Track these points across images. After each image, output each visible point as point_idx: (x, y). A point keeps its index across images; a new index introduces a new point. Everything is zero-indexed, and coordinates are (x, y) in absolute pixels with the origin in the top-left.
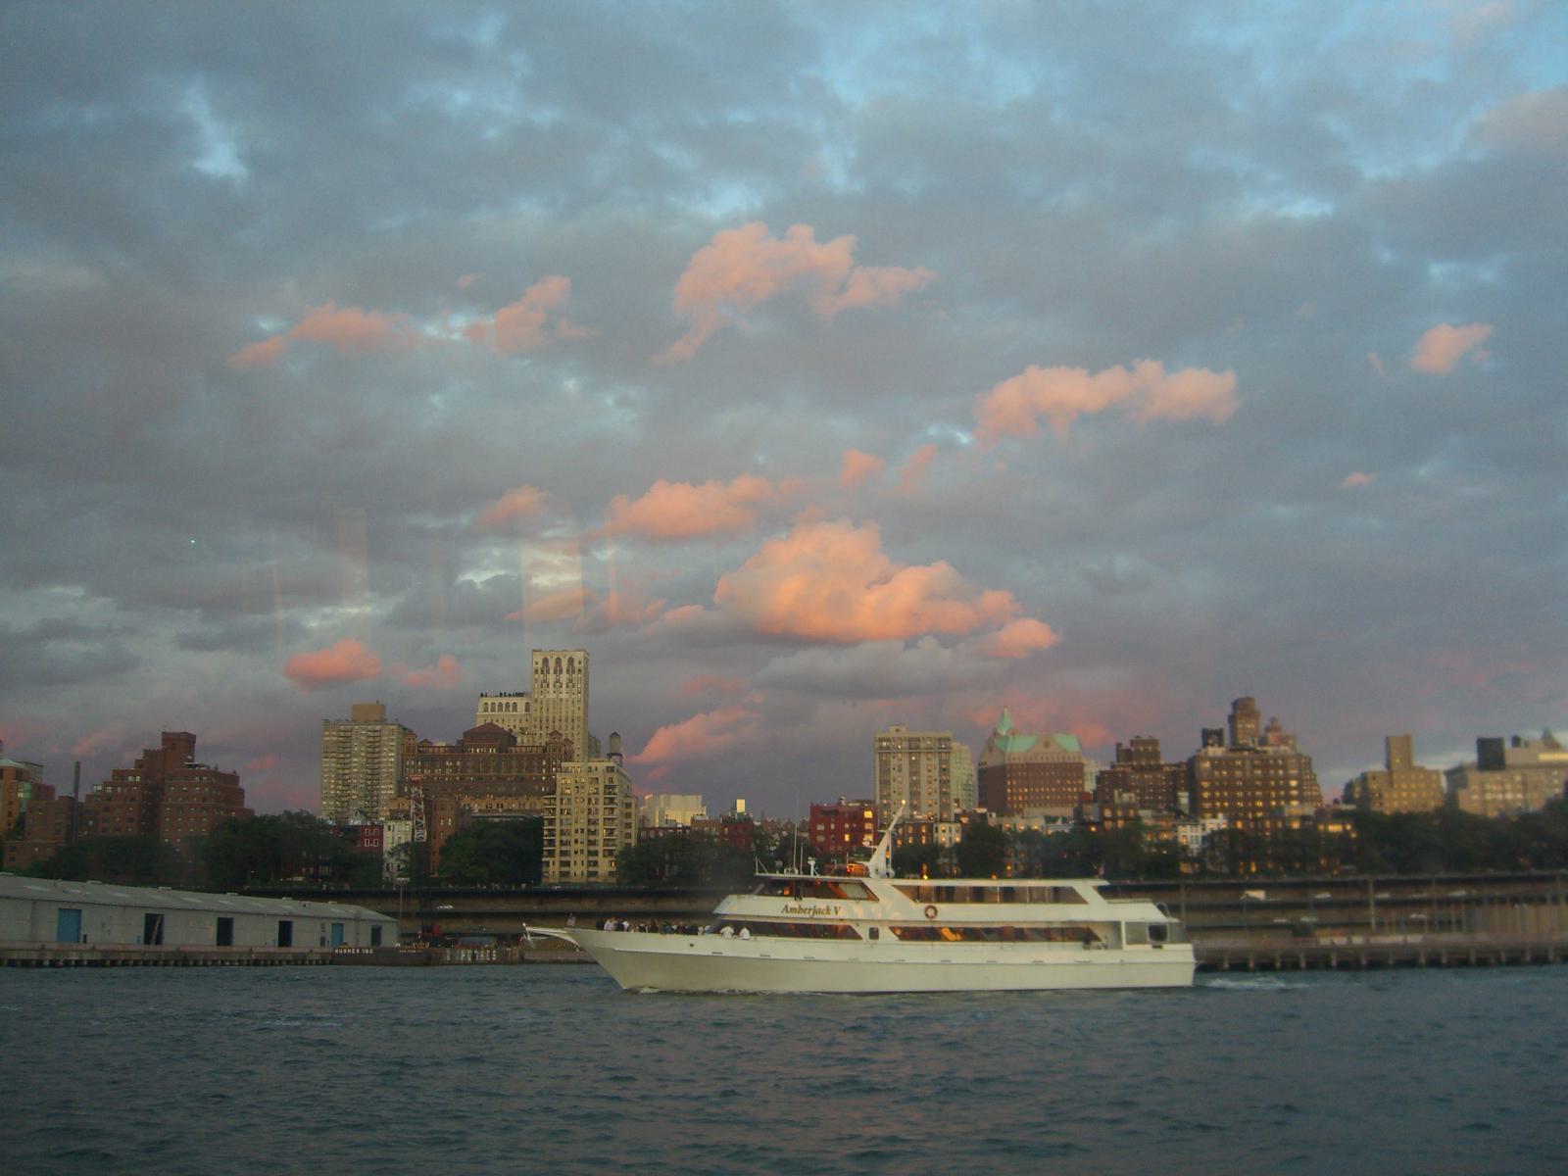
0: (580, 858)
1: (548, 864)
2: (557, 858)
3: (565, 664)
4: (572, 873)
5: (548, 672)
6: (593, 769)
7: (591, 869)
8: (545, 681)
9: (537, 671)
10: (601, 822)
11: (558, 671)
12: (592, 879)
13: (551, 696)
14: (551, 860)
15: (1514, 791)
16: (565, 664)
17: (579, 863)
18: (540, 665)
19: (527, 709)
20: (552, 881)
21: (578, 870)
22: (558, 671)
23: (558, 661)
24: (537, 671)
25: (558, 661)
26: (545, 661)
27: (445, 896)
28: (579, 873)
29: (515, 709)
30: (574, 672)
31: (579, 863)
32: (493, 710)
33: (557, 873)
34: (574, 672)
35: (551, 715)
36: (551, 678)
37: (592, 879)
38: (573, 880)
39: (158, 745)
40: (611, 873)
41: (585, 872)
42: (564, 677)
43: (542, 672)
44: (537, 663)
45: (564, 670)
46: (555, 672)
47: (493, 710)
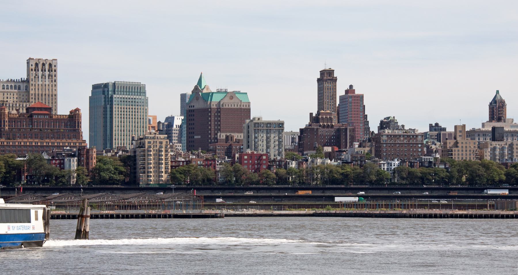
3: (47, 67)
6: (159, 138)
9: (32, 70)
11: (43, 70)
14: (144, 174)
16: (47, 67)
18: (33, 67)
22: (43, 70)
23: (44, 65)
24: (32, 70)
25: (44, 65)
26: (37, 65)
30: (52, 71)
33: (146, 180)
36: (40, 73)
43: (35, 70)
44: (32, 65)
45: (47, 70)
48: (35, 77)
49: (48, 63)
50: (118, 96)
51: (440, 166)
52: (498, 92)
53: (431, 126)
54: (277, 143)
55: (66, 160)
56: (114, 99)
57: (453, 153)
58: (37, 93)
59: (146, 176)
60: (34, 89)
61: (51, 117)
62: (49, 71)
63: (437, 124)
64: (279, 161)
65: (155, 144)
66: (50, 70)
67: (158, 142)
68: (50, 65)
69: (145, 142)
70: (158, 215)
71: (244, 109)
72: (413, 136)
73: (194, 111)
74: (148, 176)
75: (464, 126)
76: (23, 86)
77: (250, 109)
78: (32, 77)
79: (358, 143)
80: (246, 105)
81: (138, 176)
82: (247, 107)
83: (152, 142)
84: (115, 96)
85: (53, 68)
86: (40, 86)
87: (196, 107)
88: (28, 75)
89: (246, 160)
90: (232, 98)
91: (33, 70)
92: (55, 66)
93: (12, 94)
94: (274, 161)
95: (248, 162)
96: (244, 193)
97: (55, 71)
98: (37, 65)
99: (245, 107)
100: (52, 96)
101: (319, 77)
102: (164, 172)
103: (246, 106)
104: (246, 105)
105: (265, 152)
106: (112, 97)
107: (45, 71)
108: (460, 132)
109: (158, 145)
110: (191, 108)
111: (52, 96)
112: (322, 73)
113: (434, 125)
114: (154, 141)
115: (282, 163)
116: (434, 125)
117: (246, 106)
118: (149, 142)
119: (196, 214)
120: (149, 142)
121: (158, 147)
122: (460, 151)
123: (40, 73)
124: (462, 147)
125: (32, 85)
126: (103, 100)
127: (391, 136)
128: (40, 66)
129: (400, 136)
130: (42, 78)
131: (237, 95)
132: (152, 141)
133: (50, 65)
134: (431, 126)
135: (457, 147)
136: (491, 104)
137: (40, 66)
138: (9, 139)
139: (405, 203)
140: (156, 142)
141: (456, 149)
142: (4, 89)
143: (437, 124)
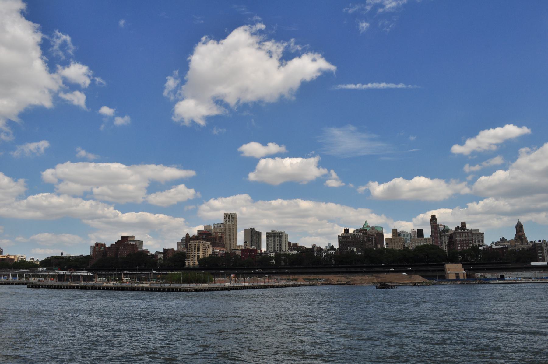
0: (192, 261)
1: (186, 263)
2: (188, 261)
3: (230, 216)
5: (227, 218)
7: (194, 264)
10: (196, 254)
11: (229, 218)
12: (194, 266)
13: (228, 224)
14: (187, 262)
15: (423, 242)
16: (230, 216)
17: (192, 262)
19: (223, 227)
21: (192, 264)
22: (229, 218)
23: (229, 216)
25: (229, 216)
26: (226, 216)
27: (222, 269)
28: (192, 265)
29: (220, 227)
31: (192, 262)
32: (216, 227)
35: (230, 228)
36: (228, 219)
37: (194, 266)
38: (191, 266)
39: (120, 239)
40: (198, 265)
42: (230, 219)
46: (228, 218)
47: (216, 227)
51: (358, 253)
52: (519, 220)
53: (501, 238)
54: (279, 244)
57: (389, 246)
58: (226, 228)
63: (503, 238)
68: (232, 216)
72: (358, 236)
75: (397, 229)
76: (222, 226)
83: (191, 245)
90: (373, 229)
99: (379, 233)
109: (194, 246)
113: (502, 238)
116: (502, 238)
118: (190, 245)
124: (394, 242)
129: (349, 237)
131: (375, 228)
133: (232, 216)
134: (501, 238)
136: (516, 226)
142: (214, 227)
143: (503, 238)
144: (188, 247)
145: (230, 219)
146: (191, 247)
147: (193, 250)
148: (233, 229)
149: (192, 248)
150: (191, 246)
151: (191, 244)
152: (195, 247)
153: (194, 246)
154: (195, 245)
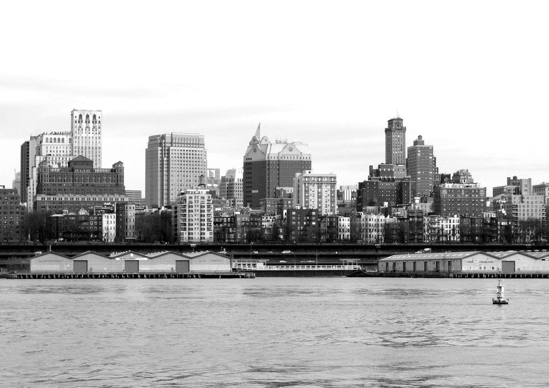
3: (91, 118)
4: (194, 238)
6: (201, 192)
8: (80, 127)
9: (76, 122)
11: (87, 122)
13: (84, 135)
14: (184, 232)
16: (91, 118)
17: (197, 234)
20: (185, 241)
22: (87, 122)
23: (88, 116)
24: (76, 122)
25: (88, 116)
26: (81, 116)
28: (197, 237)
30: (96, 122)
31: (197, 234)
33: (187, 238)
34: (96, 122)
36: (84, 125)
41: (199, 237)
42: (91, 125)
43: (79, 122)
44: (76, 117)
45: (91, 122)
47: (51, 142)
48: (79, 130)
49: (93, 114)
50: (175, 148)
54: (329, 198)
55: (104, 216)
56: (171, 152)
59: (187, 234)
60: (77, 142)
61: (92, 170)
62: (93, 122)
64: (330, 217)
65: (196, 199)
66: (94, 122)
67: (199, 197)
68: (94, 116)
69: (186, 197)
70: (184, 275)
71: (305, 162)
72: (475, 190)
73: (251, 163)
74: (189, 234)
77: (311, 162)
78: (76, 130)
79: (419, 198)
80: (274, 157)
81: (179, 233)
82: (308, 159)
83: (193, 198)
84: (171, 148)
85: (97, 118)
86: (84, 138)
87: (253, 160)
88: (72, 127)
89: (294, 216)
90: (291, 150)
91: (77, 122)
92: (99, 117)
93: (55, 147)
94: (325, 216)
95: (297, 218)
96: (267, 252)
97: (99, 122)
98: (81, 116)
100: (96, 148)
101: (387, 127)
102: (206, 229)
103: (274, 158)
104: (274, 157)
105: (316, 208)
106: (168, 150)
107: (89, 122)
108: (526, 186)
109: (200, 200)
110: (248, 161)
111: (96, 148)
112: (390, 122)
114: (195, 196)
115: (333, 219)
117: (274, 158)
119: (209, 274)
120: (191, 198)
121: (200, 202)
122: (526, 207)
123: (84, 125)
125: (76, 137)
126: (159, 152)
127: (451, 190)
128: (84, 118)
129: (461, 190)
130: (86, 130)
132: (193, 196)
133: (94, 116)
135: (522, 202)
137: (84, 118)
138: (50, 195)
139: (24, 274)
140: (198, 196)
141: (522, 204)
144: (187, 202)
145: (91, 125)
146: (193, 202)
147: (199, 208)
148: (98, 150)
149: (197, 204)
150: (193, 200)
151: (193, 196)
152: (203, 202)
153: (200, 200)
154: (203, 198)
